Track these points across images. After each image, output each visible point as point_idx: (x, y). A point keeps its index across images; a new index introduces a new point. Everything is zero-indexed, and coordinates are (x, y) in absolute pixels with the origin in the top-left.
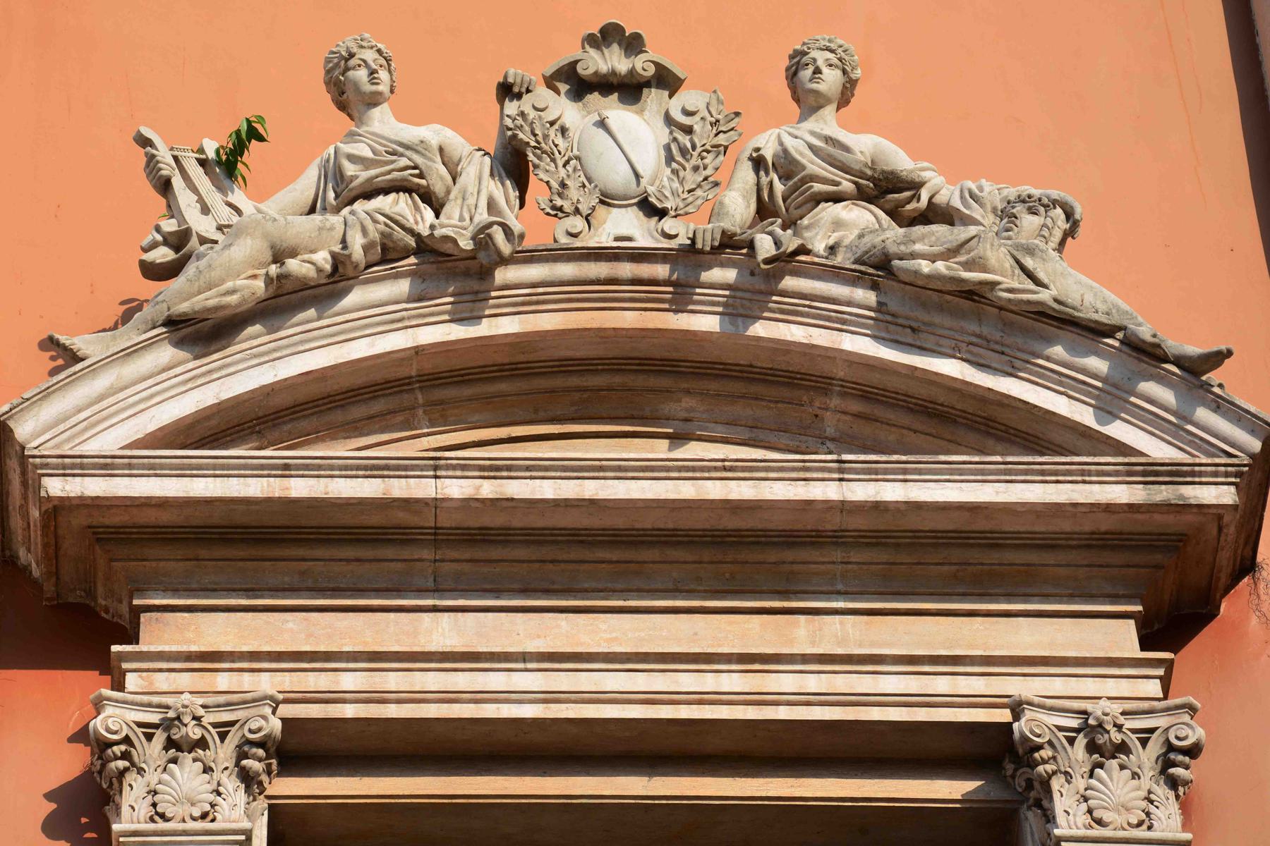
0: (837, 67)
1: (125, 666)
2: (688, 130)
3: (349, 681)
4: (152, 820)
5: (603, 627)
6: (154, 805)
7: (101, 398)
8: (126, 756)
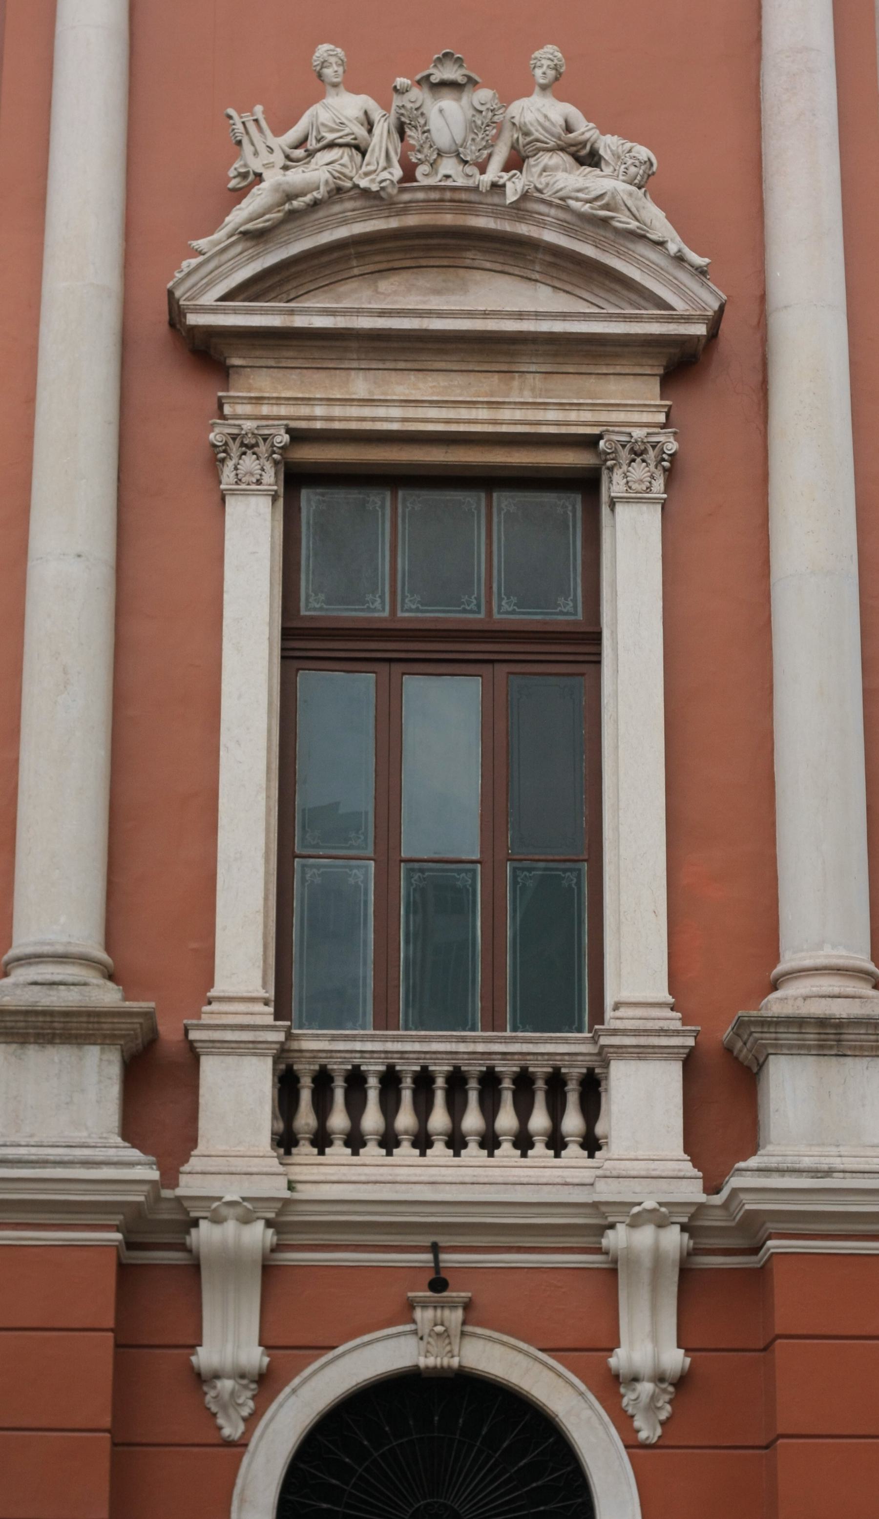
0: (553, 69)
1: (223, 401)
2: (481, 112)
3: (319, 411)
4: (237, 483)
5: (430, 379)
6: (237, 475)
7: (212, 272)
8: (225, 451)
